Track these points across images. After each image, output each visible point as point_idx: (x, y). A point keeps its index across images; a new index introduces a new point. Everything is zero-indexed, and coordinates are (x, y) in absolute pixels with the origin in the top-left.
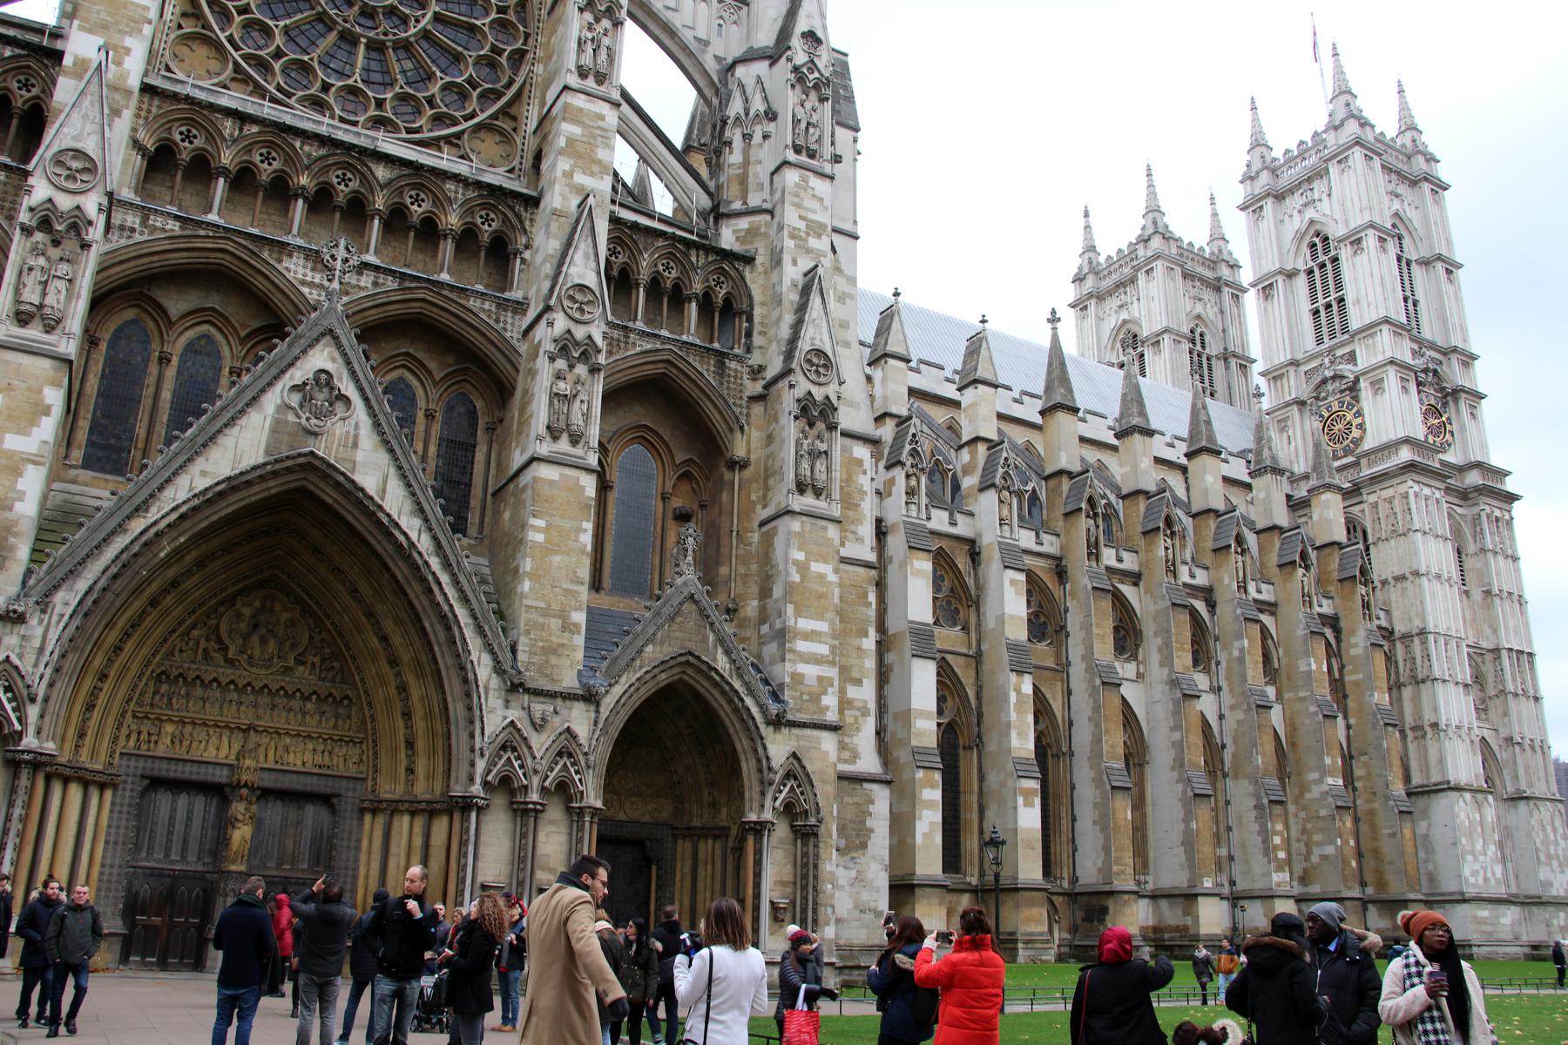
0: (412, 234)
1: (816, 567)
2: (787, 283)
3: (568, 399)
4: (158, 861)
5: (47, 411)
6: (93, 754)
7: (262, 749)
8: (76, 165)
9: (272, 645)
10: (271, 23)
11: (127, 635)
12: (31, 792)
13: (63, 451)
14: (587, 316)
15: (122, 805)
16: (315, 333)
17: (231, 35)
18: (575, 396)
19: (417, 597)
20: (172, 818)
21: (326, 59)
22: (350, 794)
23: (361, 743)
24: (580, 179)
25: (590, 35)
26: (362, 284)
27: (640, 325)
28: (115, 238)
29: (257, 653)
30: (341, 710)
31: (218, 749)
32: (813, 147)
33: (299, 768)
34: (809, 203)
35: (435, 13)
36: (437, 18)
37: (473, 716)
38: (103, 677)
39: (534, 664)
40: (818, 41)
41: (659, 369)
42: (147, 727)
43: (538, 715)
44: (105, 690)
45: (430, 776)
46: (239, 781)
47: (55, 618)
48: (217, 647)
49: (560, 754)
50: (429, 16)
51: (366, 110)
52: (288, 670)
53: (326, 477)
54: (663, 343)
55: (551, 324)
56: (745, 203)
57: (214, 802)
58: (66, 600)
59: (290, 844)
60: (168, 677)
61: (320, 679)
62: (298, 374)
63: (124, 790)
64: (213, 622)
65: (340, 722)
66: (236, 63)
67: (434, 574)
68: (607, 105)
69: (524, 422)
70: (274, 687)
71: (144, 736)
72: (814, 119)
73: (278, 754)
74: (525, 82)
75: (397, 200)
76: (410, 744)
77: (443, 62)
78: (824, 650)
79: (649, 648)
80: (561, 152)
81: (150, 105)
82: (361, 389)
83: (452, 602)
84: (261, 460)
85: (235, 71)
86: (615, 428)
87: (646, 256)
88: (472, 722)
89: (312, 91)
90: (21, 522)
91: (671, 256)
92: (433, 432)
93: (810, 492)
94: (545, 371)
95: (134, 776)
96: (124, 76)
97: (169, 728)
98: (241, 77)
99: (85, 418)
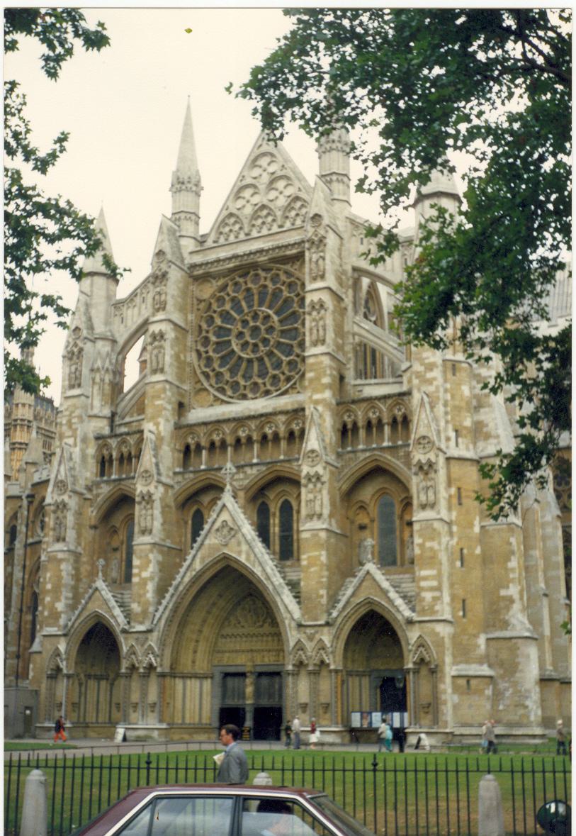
1: (428, 544)
3: (313, 501)
5: (150, 561)
25: (314, 324)
27: (361, 447)
38: (197, 641)
41: (374, 464)
42: (220, 655)
52: (261, 626)
58: (163, 621)
62: (218, 524)
78: (435, 583)
96: (159, 433)
97: (227, 655)
98: (217, 399)
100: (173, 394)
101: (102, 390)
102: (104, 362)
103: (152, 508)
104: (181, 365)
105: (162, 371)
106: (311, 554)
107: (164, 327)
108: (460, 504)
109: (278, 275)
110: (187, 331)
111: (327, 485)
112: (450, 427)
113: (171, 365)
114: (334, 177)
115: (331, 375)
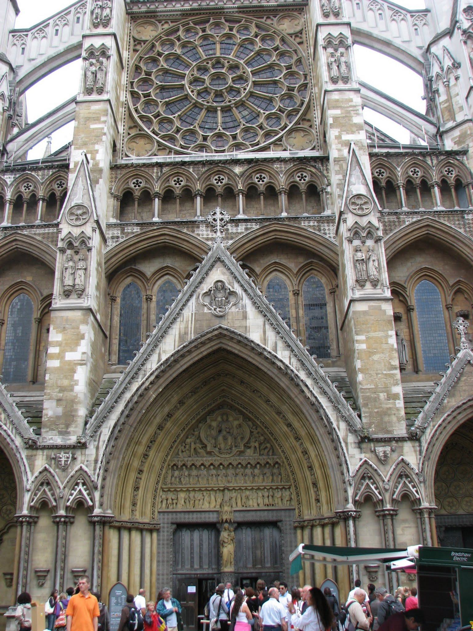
0: (262, 197)
4: (188, 570)
5: (83, 337)
6: (142, 514)
7: (234, 499)
8: (80, 212)
9: (230, 440)
10: (171, 117)
11: (149, 447)
12: (103, 537)
13: (107, 358)
14: (366, 211)
15: (163, 540)
16: (212, 261)
17: (153, 129)
18: (369, 258)
19: (296, 396)
20: (192, 545)
21: (203, 124)
22: (288, 519)
23: (289, 488)
24: (346, 137)
25: (333, 60)
26: (239, 231)
27: (405, 209)
28: (110, 244)
29: (222, 446)
30: (275, 471)
31: (209, 503)
33: (256, 508)
35: (254, 82)
36: (255, 84)
37: (341, 462)
38: (141, 471)
39: (374, 423)
41: (424, 232)
42: (170, 496)
43: (381, 454)
44: (143, 479)
45: (329, 502)
46: (222, 520)
47: (101, 443)
48: (200, 446)
49: (400, 476)
50: (250, 84)
51: (228, 143)
52: (241, 453)
53: (232, 338)
54: (422, 216)
55: (345, 221)
57: (213, 533)
58: (106, 432)
59: (258, 552)
60: (177, 467)
61: (260, 455)
63: (163, 532)
64: (196, 433)
65: (275, 478)
66: (158, 142)
67: (302, 381)
69: (345, 282)
70: (235, 463)
71: (170, 501)
73: (243, 501)
74: (310, 100)
75: (250, 181)
76: (315, 484)
77: (264, 105)
79: (446, 401)
81: (116, 174)
82: (242, 286)
83: (316, 395)
84: (193, 338)
85: (159, 146)
86: (407, 274)
87: (399, 169)
88: (341, 465)
89: (198, 142)
90: (79, 396)
91: (415, 165)
92: (300, 302)
94: (348, 250)
95: (168, 523)
96: (97, 164)
97: (182, 495)
98: (162, 148)
99: (115, 338)
103: (85, 259)
105: (101, 91)
106: (372, 334)
107: (109, 42)
109: (246, 28)
110: (123, 68)
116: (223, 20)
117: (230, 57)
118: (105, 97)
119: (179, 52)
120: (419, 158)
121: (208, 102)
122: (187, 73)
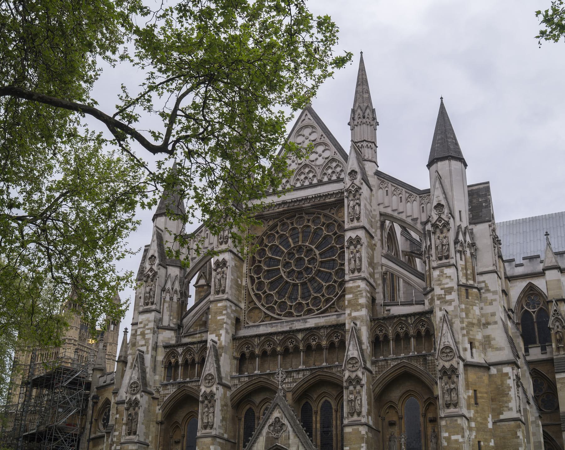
1: (454, 437)
2: (438, 319)
10: (272, 293)
24: (354, 314)
25: (352, 256)
27: (391, 356)
32: (446, 254)
34: (444, 281)
40: (443, 206)
41: (403, 370)
56: (431, 287)
68: (360, 281)
72: (445, 241)
80: (347, 307)
92: (338, 416)
93: (452, 406)
96: (221, 343)
100: (233, 311)
101: (170, 306)
102: (173, 284)
104: (239, 287)
105: (224, 292)
107: (227, 256)
108: (476, 404)
109: (319, 218)
111: (365, 387)
112: (466, 339)
113: (231, 287)
114: (365, 144)
115: (366, 297)
116: (304, 215)
117: (307, 244)
118: (225, 296)
119: (277, 243)
120: (404, 319)
121: (293, 280)
122: (281, 259)
